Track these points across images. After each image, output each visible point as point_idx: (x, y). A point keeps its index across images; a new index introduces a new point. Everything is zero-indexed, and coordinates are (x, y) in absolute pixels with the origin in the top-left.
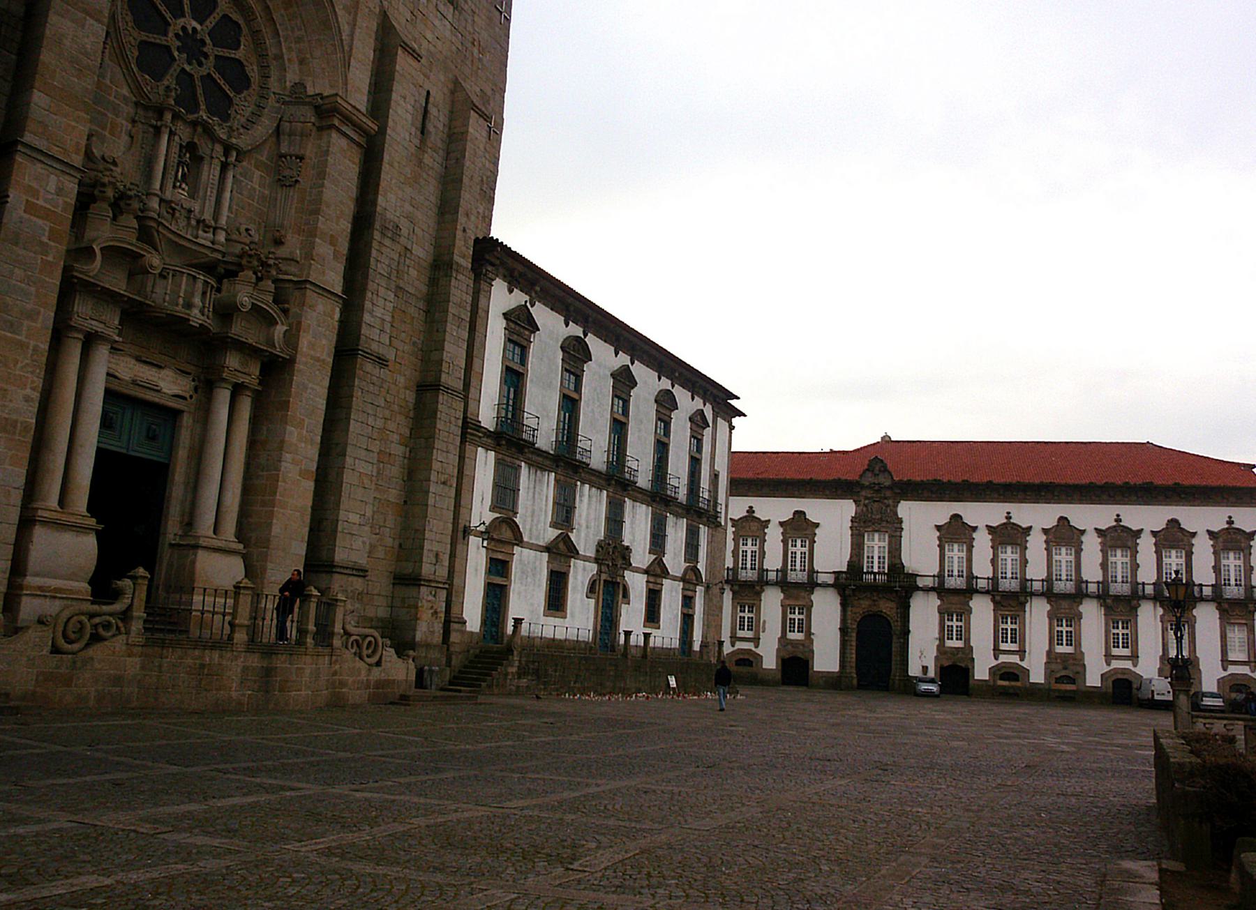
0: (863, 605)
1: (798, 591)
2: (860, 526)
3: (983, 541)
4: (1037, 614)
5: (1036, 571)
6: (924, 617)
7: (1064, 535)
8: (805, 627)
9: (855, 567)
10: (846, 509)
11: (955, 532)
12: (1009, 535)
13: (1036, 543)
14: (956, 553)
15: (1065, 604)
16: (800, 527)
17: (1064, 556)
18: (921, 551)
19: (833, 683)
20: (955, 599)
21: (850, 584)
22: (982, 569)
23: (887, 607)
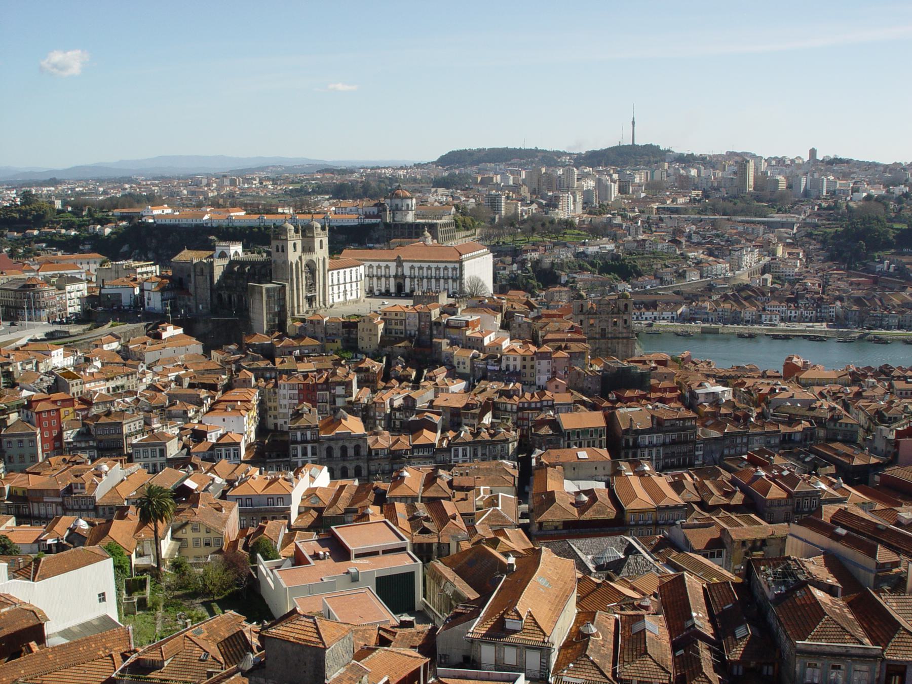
0: (398, 281)
2: (397, 266)
3: (417, 269)
4: (425, 280)
5: (425, 275)
6: (408, 281)
7: (429, 268)
10: (395, 264)
11: (412, 268)
12: (421, 268)
13: (425, 269)
16: (387, 267)
17: (429, 272)
18: (407, 272)
20: (412, 278)
21: (396, 277)
23: (401, 281)
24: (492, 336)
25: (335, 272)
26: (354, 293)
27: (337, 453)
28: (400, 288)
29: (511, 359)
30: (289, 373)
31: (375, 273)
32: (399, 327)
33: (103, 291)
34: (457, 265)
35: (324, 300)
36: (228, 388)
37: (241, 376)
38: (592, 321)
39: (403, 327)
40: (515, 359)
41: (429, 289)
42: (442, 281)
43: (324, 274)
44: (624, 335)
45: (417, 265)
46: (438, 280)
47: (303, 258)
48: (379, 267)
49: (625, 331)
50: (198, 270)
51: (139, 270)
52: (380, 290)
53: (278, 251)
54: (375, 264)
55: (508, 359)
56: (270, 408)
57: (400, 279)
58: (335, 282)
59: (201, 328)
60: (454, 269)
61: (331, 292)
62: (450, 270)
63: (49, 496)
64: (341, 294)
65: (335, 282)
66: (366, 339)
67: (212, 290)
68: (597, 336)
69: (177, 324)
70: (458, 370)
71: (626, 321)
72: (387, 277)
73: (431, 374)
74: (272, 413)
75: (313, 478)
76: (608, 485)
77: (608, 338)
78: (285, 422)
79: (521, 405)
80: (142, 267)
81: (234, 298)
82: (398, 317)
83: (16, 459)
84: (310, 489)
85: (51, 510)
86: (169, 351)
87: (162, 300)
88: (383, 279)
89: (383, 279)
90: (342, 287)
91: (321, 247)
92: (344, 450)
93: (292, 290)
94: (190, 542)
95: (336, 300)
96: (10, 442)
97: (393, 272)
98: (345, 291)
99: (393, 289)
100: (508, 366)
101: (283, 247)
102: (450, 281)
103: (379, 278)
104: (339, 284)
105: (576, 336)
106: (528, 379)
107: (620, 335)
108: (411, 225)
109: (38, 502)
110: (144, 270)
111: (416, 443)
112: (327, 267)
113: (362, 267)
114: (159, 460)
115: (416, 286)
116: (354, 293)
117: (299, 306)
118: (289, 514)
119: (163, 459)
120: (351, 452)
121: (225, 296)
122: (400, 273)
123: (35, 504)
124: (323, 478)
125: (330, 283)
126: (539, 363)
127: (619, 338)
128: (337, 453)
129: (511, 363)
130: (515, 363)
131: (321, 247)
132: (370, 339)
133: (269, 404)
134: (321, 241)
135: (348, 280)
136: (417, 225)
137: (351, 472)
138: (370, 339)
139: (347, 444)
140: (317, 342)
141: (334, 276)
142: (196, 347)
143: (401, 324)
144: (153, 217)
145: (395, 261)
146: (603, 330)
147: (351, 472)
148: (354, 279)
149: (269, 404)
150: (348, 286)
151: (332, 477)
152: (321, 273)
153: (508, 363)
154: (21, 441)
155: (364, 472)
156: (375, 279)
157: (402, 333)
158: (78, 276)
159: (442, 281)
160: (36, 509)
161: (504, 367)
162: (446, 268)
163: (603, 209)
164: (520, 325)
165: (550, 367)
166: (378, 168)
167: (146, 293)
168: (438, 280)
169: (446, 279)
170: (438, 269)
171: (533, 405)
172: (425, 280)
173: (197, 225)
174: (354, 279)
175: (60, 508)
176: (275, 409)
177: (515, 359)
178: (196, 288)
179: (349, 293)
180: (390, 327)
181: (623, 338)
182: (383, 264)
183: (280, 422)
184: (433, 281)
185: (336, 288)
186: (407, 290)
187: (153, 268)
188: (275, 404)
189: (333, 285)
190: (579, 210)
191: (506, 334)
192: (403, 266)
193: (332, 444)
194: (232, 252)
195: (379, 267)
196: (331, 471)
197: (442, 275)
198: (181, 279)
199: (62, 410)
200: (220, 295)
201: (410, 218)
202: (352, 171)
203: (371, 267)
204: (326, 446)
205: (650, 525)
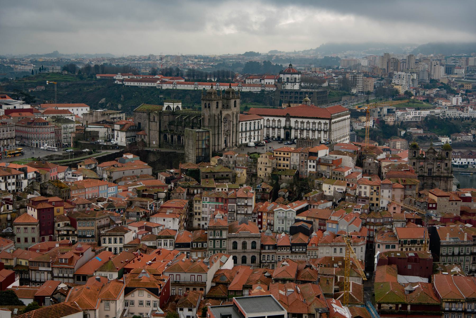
1: (279, 129)
2: (286, 121)
4: (305, 131)
5: (305, 127)
6: (293, 132)
7: (308, 123)
8: (280, 133)
9: (285, 126)
11: (296, 122)
12: (302, 122)
13: (305, 124)
14: (297, 124)
15: (308, 131)
16: (279, 121)
18: (293, 125)
19: (283, 140)
20: (296, 130)
21: (285, 128)
22: (299, 126)
23: (289, 131)
24: (350, 171)
25: (244, 123)
26: (256, 138)
27: (240, 246)
28: (288, 135)
29: (363, 186)
30: (209, 189)
31: (271, 125)
32: (286, 162)
33: (88, 129)
34: (328, 121)
35: (236, 142)
36: (168, 198)
37: (178, 190)
38: (422, 163)
39: (288, 162)
40: (365, 188)
41: (308, 138)
42: (316, 132)
43: (237, 124)
44: (446, 175)
45: (300, 120)
46: (313, 131)
47: (223, 112)
48: (274, 121)
49: (445, 172)
50: (152, 118)
51: (111, 116)
52: (273, 137)
53: (206, 107)
54: (271, 118)
55: (361, 187)
56: (196, 213)
57: (288, 129)
58: (244, 130)
59: (152, 158)
60: (325, 124)
61: (240, 137)
62: (323, 125)
63: (44, 266)
64: (247, 138)
65: (244, 130)
66: (263, 169)
67: (160, 132)
68: (426, 174)
69: (136, 153)
70: (326, 194)
71: (446, 164)
72: (279, 129)
73: (306, 195)
74: (197, 216)
75: (222, 264)
76: (430, 281)
77: (433, 177)
78: (206, 224)
79: (368, 220)
80: (113, 114)
81: (175, 137)
82: (286, 156)
83: (22, 240)
84: (219, 270)
85: (44, 277)
86: (128, 173)
87: (127, 137)
88: (276, 130)
89: (276, 130)
90: (248, 134)
91: (235, 106)
92: (244, 244)
93: (215, 134)
94: (136, 303)
95: (244, 142)
96: (18, 228)
97: (283, 124)
98: (250, 136)
99: (282, 136)
100: (360, 193)
101: (209, 104)
102: (322, 132)
103: (273, 129)
104: (246, 131)
105: (408, 173)
106: (374, 201)
107: (442, 175)
108: (296, 92)
109: (35, 270)
110: (115, 116)
111: (295, 241)
112: (238, 120)
113: (262, 120)
114: (119, 245)
115: (299, 135)
116: (256, 138)
117: (218, 145)
118: (205, 287)
119: (122, 245)
120: (249, 246)
121: (169, 136)
122: (288, 126)
123: (33, 272)
124: (229, 265)
125: (240, 131)
126: (383, 191)
127: (440, 177)
128: (240, 246)
129: (363, 190)
130: (365, 190)
131: (235, 106)
132: (266, 169)
133: (195, 211)
134: (235, 101)
135: (252, 128)
136: (301, 93)
137: (249, 260)
138: (266, 169)
139: (247, 241)
140: (229, 170)
141: (242, 126)
142: (148, 170)
143: (287, 160)
144: (122, 81)
145: (283, 117)
146: (430, 170)
147: (249, 260)
148: (256, 128)
149: (195, 211)
150: (252, 133)
151: (235, 262)
152: (235, 123)
153: (361, 190)
154: (26, 228)
155: (258, 261)
156: (271, 129)
157: (287, 166)
158: (70, 118)
159: (316, 132)
160: (33, 276)
161: (357, 192)
162: (320, 123)
163: (433, 83)
164: (370, 164)
165: (390, 194)
166: (276, 51)
167: (116, 133)
168: (313, 131)
169: (319, 131)
170: (314, 123)
171: (378, 221)
172: (305, 132)
173: (152, 87)
174: (256, 128)
175: (50, 276)
176: (199, 214)
177: (365, 188)
178: (149, 130)
179: (253, 138)
180: (279, 162)
181: (444, 177)
182: (276, 119)
183: (202, 223)
184: (310, 131)
185: (244, 135)
186: (293, 136)
187: (121, 115)
188: (199, 211)
189: (242, 132)
190: (416, 85)
191: (360, 170)
192: (290, 121)
193: (237, 240)
194: (175, 107)
195: (274, 121)
196: (235, 259)
197: (317, 128)
198: (139, 124)
199: (55, 209)
200: (165, 136)
201: (297, 87)
202: (258, 54)
203: (268, 120)
204: (233, 241)
205: (459, 311)
